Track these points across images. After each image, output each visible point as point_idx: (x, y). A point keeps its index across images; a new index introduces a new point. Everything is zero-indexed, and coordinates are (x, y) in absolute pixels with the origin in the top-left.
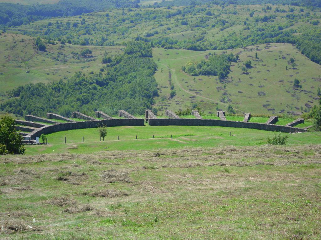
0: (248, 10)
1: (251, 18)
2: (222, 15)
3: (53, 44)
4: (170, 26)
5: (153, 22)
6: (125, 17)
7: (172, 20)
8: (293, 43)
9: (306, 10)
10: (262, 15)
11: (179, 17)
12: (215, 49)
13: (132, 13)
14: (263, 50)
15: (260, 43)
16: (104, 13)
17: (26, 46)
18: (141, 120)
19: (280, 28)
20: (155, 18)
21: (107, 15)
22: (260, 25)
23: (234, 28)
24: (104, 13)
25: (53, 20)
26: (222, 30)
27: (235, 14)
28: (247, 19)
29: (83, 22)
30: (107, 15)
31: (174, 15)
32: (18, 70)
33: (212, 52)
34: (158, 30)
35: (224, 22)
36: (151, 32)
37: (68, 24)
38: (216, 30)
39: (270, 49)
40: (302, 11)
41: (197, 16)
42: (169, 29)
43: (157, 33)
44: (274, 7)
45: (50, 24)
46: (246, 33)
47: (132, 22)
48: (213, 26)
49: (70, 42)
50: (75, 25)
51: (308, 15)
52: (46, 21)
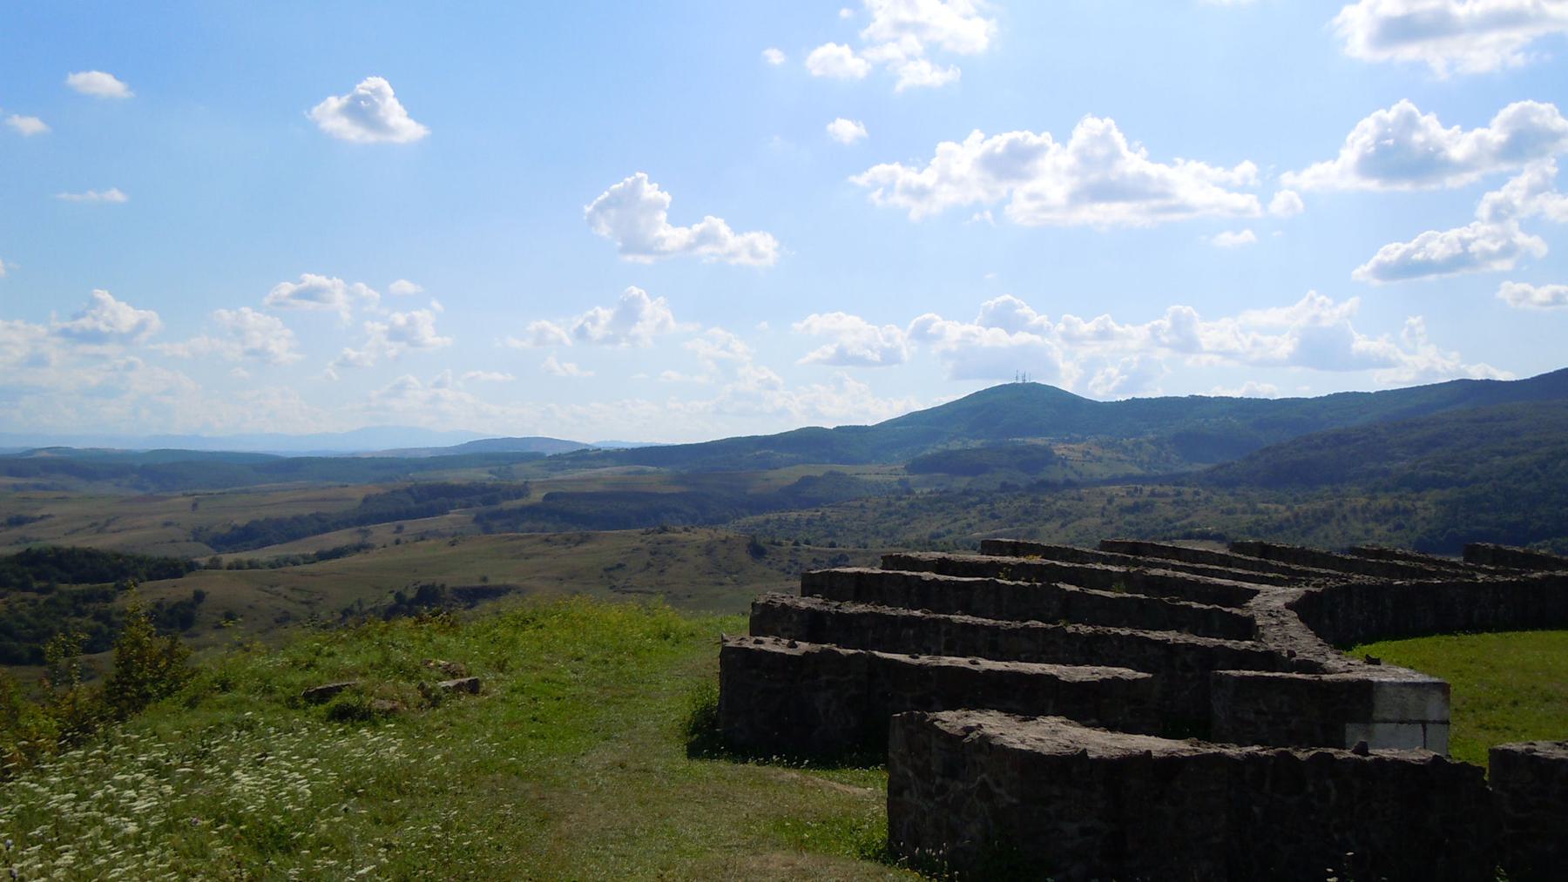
0: (1102, 494)
2: (1059, 503)
5: (939, 516)
7: (974, 512)
8: (1219, 538)
9: (1204, 494)
10: (1129, 502)
11: (986, 507)
13: (903, 503)
16: (857, 504)
20: (942, 509)
21: (862, 506)
22: (1129, 517)
24: (857, 504)
25: (773, 516)
27: (1080, 499)
29: (822, 518)
31: (974, 504)
32: (717, 589)
34: (951, 527)
35: (1062, 513)
36: (941, 531)
37: (797, 520)
40: (1197, 493)
41: (1016, 504)
42: (970, 526)
43: (949, 532)
44: (1147, 489)
45: (768, 521)
47: (905, 516)
48: (1047, 520)
49: (807, 542)
50: (809, 522)
51: (1207, 500)
52: (761, 518)
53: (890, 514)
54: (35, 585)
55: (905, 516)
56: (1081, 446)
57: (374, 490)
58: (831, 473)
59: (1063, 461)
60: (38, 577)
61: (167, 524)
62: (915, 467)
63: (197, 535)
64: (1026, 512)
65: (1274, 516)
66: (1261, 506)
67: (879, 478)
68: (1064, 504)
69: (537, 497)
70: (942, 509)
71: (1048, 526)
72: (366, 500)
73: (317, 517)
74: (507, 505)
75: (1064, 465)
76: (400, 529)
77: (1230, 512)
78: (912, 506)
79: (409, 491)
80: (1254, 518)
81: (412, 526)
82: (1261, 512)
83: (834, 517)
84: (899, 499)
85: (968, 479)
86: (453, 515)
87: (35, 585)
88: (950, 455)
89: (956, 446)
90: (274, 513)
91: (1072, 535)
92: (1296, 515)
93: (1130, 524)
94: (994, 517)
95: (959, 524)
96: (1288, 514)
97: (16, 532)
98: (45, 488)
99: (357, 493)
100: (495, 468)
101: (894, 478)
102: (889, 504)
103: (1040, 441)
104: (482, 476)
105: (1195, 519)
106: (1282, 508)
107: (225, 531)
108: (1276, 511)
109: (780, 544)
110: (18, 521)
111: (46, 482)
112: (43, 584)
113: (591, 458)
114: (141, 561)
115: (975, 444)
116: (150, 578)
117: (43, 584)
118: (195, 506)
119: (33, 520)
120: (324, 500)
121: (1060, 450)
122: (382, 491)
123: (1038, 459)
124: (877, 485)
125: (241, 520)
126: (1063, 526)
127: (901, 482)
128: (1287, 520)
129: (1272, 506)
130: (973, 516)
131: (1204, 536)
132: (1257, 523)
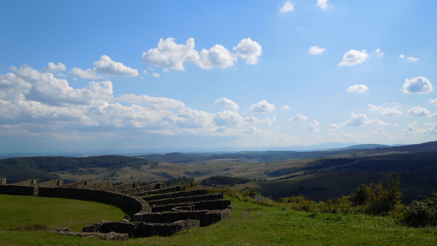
54: (212, 185)
57: (311, 160)
60: (213, 183)
61: (259, 170)
63: (266, 173)
72: (308, 163)
73: (295, 168)
79: (320, 161)
87: (212, 185)
90: (284, 167)
97: (226, 172)
98: (239, 161)
99: (307, 161)
104: (347, 156)
107: (273, 172)
110: (227, 169)
111: (239, 160)
112: (214, 185)
113: (381, 150)
114: (236, 179)
116: (238, 183)
117: (214, 185)
118: (267, 165)
119: (230, 169)
120: (298, 163)
122: (313, 161)
125: (276, 169)
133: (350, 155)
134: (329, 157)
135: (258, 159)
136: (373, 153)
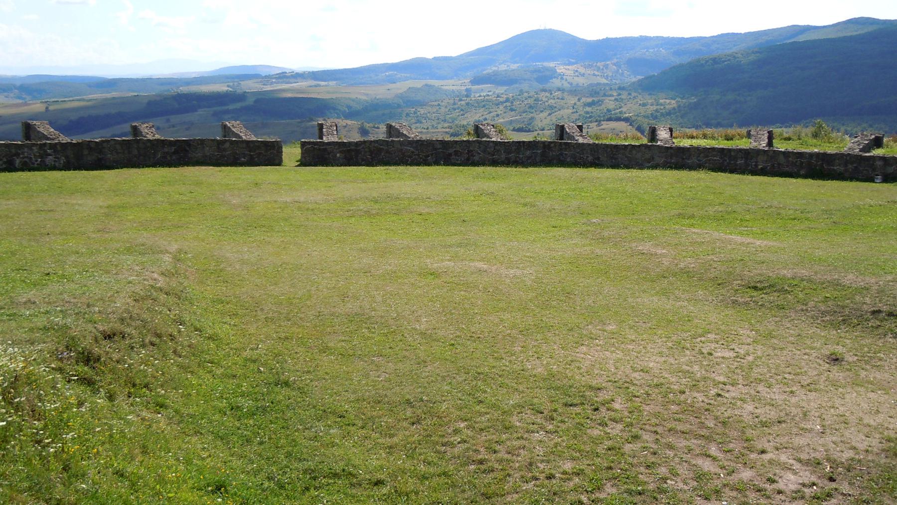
1: (578, 103)
3: (378, 128)
4: (499, 112)
6: (456, 106)
7: (501, 107)
8: (626, 120)
11: (508, 104)
12: (543, 130)
13: (463, 103)
14: (595, 128)
15: (591, 122)
16: (436, 103)
17: (349, 131)
18: (265, 144)
19: (609, 110)
20: (484, 106)
21: (439, 105)
22: (588, 109)
23: (561, 112)
24: (436, 103)
26: (550, 114)
27: (562, 99)
28: (575, 104)
29: (415, 113)
30: (439, 105)
31: (502, 103)
33: (541, 132)
34: (487, 117)
35: (551, 107)
38: (545, 114)
39: (602, 127)
42: (498, 115)
46: (576, 116)
47: (462, 110)
48: (542, 112)
53: (455, 109)
55: (462, 110)
56: (574, 67)
58: (426, 85)
59: (562, 76)
62: (476, 81)
64: (531, 107)
65: (667, 107)
66: (661, 101)
67: (454, 88)
68: (552, 101)
69: (250, 101)
70: (484, 106)
71: (541, 115)
74: (231, 107)
75: (562, 78)
76: (168, 121)
77: (644, 105)
78: (467, 104)
80: (655, 108)
81: (175, 119)
82: (662, 105)
83: (422, 111)
84: (461, 100)
85: (506, 88)
86: (201, 112)
88: (496, 74)
89: (503, 67)
91: (554, 120)
92: (679, 106)
93: (587, 113)
94: (512, 110)
95: (492, 114)
96: (675, 105)
100: (231, 84)
101: (464, 88)
102: (454, 104)
103: (552, 65)
104: (222, 88)
105: (624, 109)
106: (673, 102)
108: (669, 104)
109: (378, 128)
115: (514, 66)
121: (561, 69)
123: (544, 76)
124: (453, 91)
126: (550, 114)
127: (467, 90)
128: (674, 109)
129: (668, 101)
130: (500, 110)
131: (618, 119)
132: (657, 111)
133: (228, 86)
134: (184, 89)
135: (12, 95)
136: (272, 83)
